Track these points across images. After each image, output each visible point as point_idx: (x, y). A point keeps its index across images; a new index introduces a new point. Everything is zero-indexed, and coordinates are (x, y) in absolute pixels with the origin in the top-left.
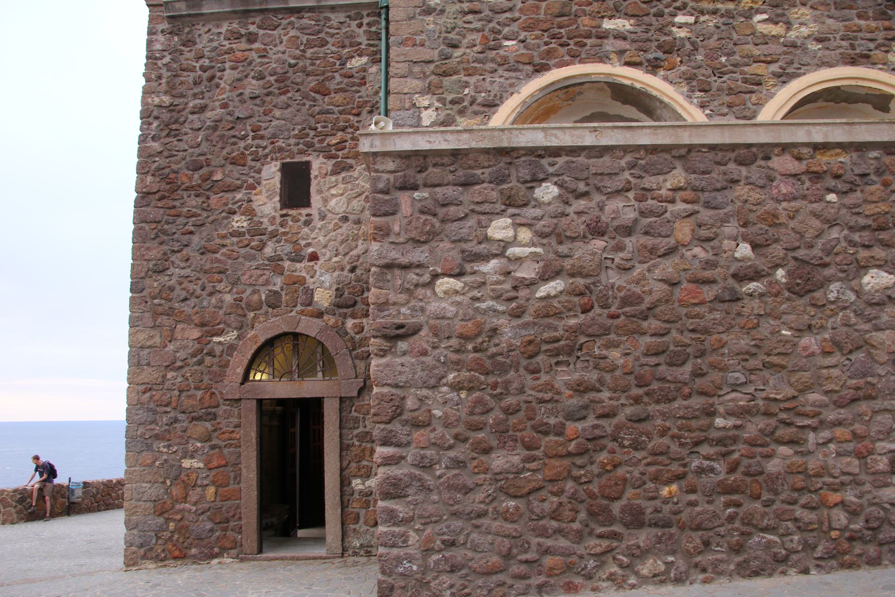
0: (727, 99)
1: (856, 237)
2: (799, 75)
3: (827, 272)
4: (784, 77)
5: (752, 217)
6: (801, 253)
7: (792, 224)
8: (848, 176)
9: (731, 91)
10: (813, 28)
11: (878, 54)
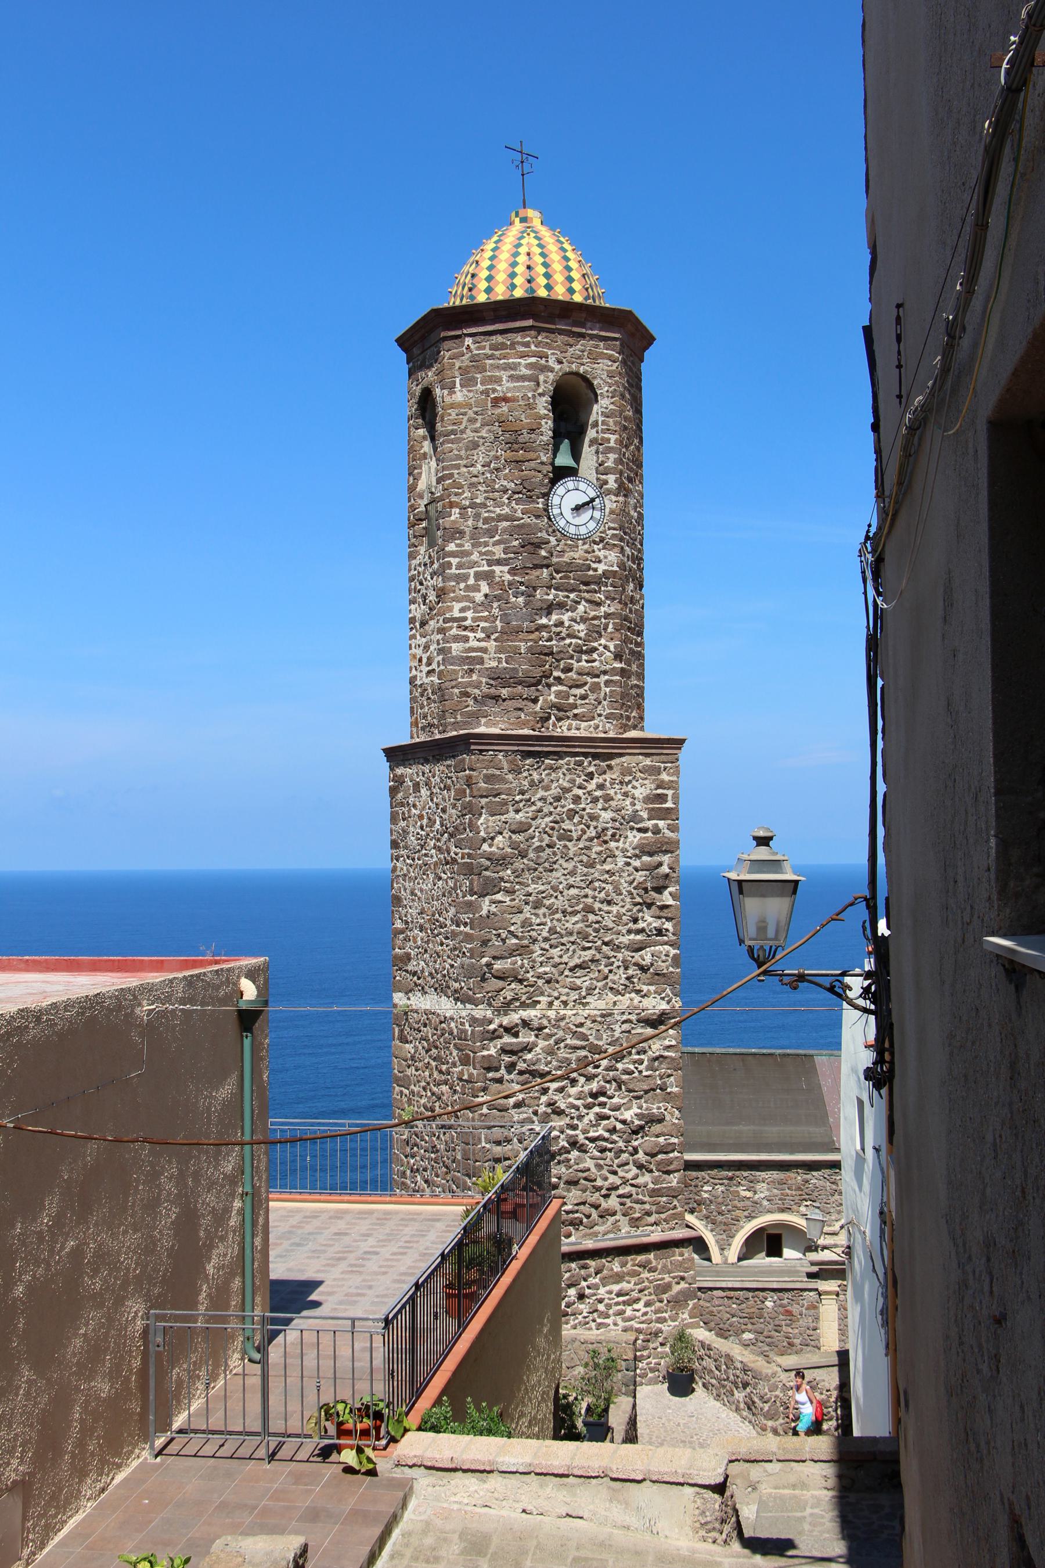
0: (724, 1228)
1: (741, 1321)
2: (756, 1217)
3: (731, 1333)
4: (749, 1218)
5: (704, 1313)
6: (721, 1326)
7: (719, 1315)
8: (741, 1298)
9: (725, 1224)
10: (767, 1193)
11: (795, 1207)
